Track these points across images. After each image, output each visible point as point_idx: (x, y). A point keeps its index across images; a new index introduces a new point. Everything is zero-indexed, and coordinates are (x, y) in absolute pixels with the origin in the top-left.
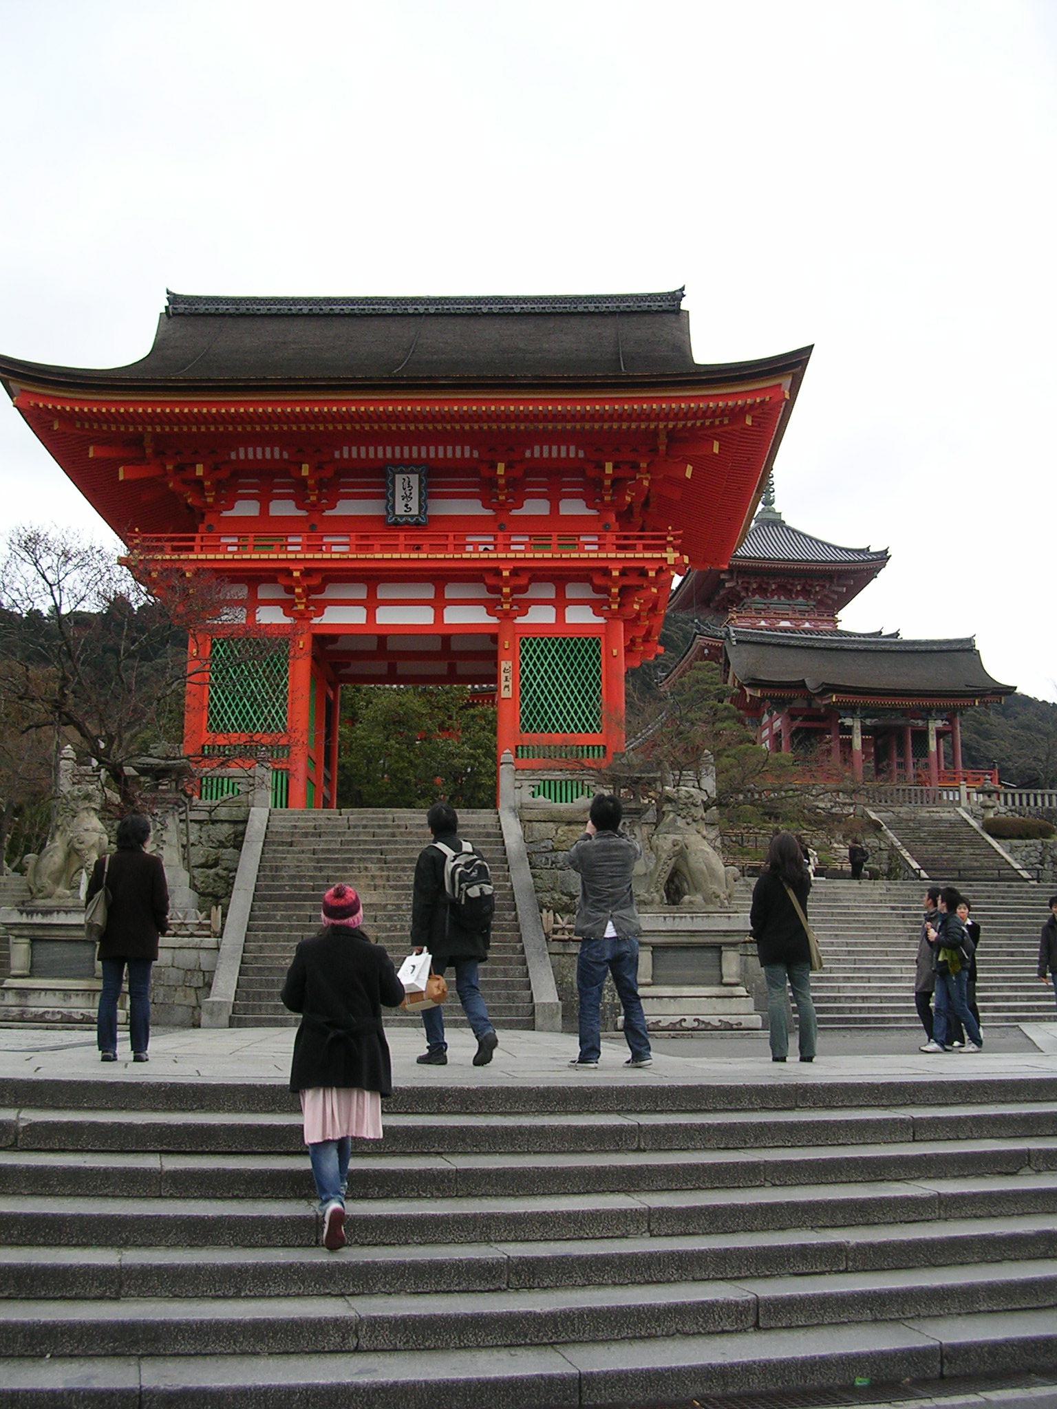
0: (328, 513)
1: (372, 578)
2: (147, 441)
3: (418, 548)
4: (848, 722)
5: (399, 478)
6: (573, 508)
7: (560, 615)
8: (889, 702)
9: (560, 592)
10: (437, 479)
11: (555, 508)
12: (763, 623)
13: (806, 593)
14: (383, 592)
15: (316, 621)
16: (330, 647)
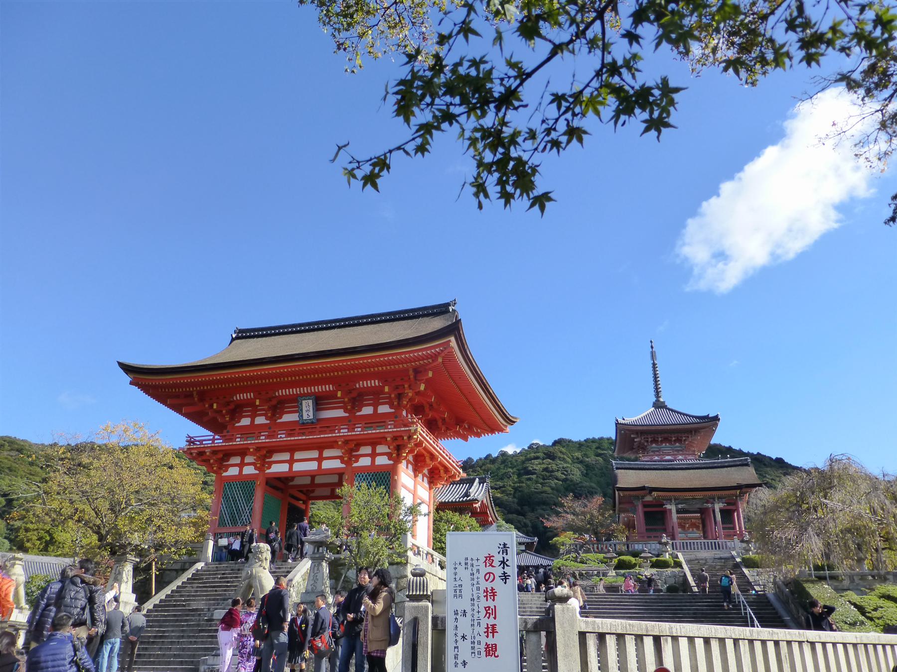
0: (279, 421)
1: (292, 449)
2: (195, 394)
3: (303, 434)
4: (668, 507)
5: (304, 402)
6: (384, 409)
7: (373, 461)
8: (688, 495)
9: (374, 450)
10: (320, 402)
11: (375, 410)
12: (656, 458)
13: (679, 440)
14: (298, 455)
15: (268, 471)
16: (291, 483)
